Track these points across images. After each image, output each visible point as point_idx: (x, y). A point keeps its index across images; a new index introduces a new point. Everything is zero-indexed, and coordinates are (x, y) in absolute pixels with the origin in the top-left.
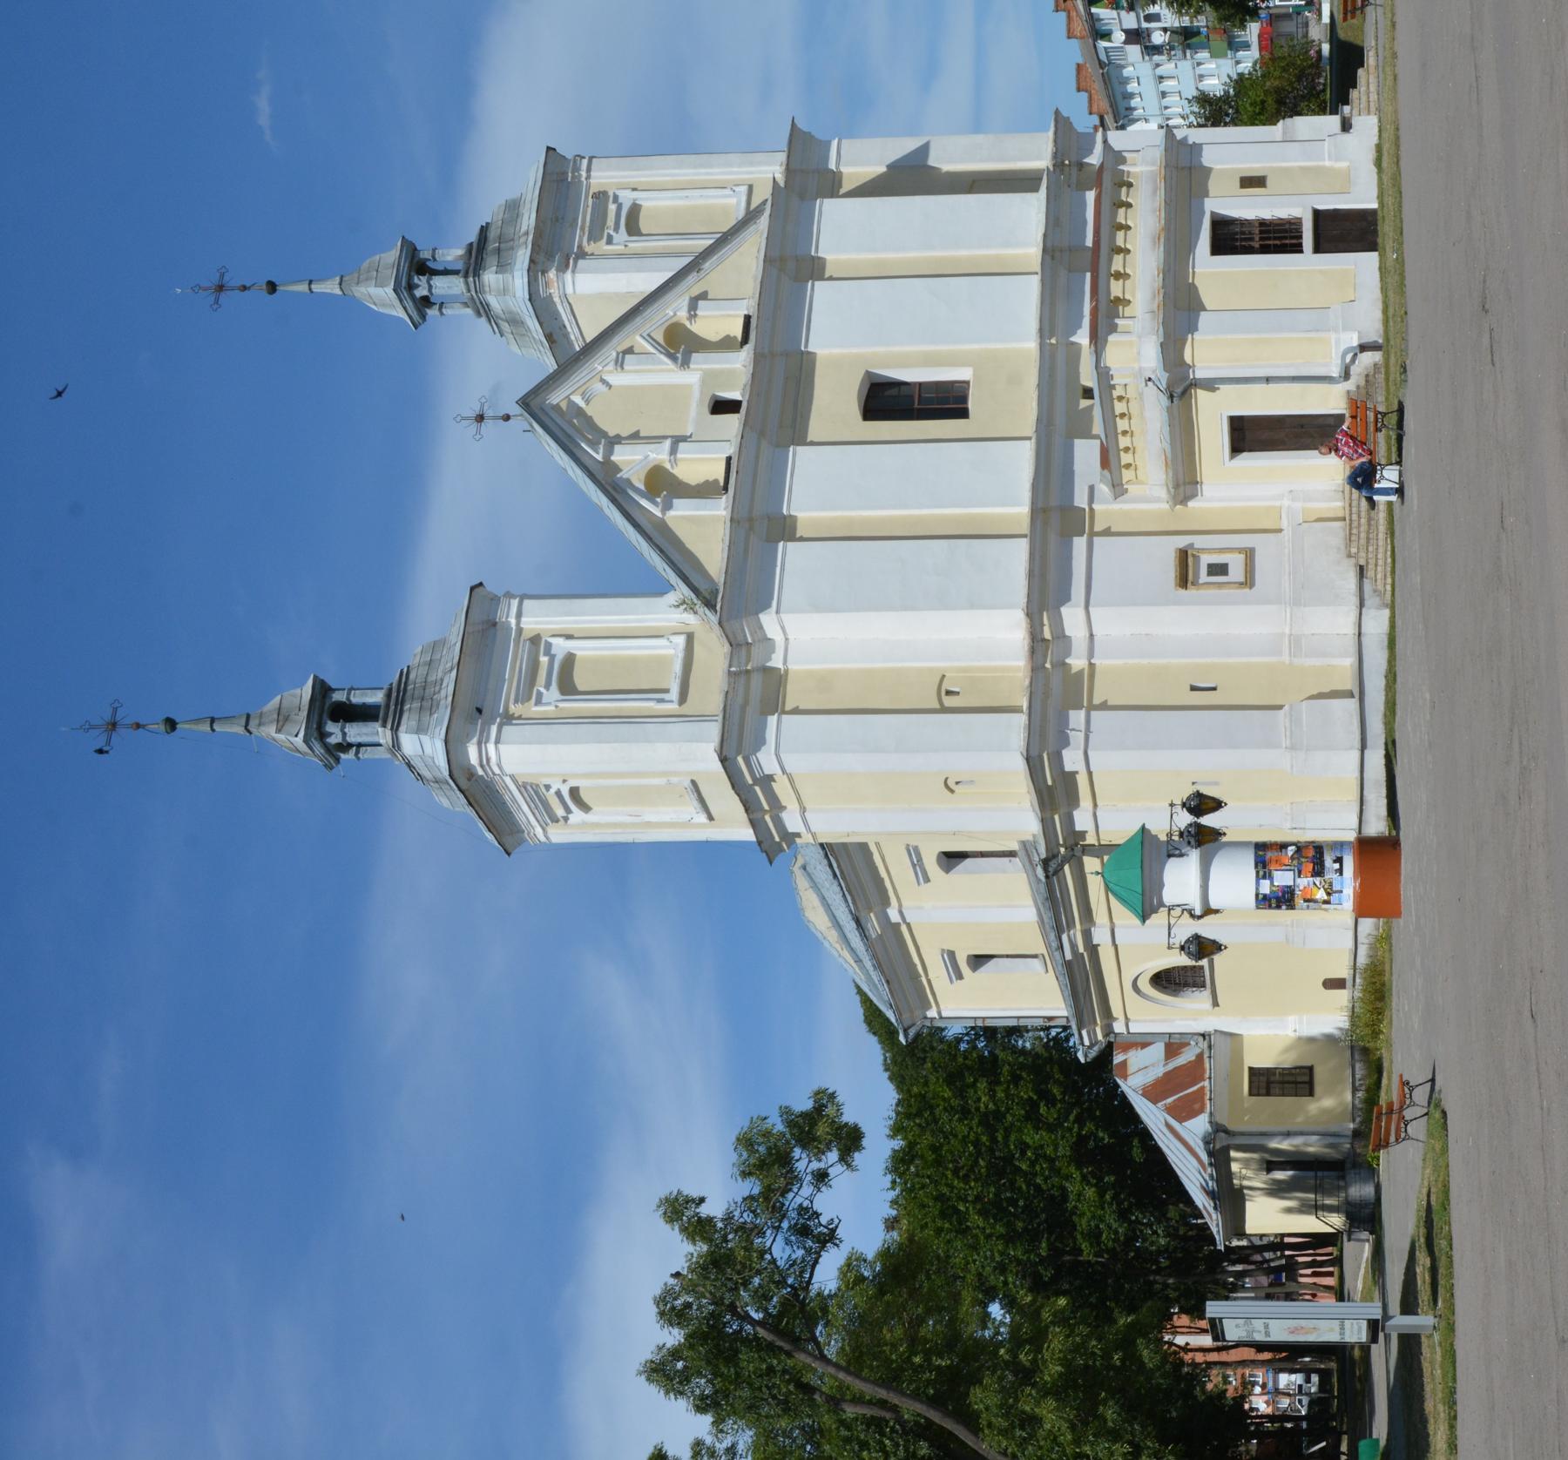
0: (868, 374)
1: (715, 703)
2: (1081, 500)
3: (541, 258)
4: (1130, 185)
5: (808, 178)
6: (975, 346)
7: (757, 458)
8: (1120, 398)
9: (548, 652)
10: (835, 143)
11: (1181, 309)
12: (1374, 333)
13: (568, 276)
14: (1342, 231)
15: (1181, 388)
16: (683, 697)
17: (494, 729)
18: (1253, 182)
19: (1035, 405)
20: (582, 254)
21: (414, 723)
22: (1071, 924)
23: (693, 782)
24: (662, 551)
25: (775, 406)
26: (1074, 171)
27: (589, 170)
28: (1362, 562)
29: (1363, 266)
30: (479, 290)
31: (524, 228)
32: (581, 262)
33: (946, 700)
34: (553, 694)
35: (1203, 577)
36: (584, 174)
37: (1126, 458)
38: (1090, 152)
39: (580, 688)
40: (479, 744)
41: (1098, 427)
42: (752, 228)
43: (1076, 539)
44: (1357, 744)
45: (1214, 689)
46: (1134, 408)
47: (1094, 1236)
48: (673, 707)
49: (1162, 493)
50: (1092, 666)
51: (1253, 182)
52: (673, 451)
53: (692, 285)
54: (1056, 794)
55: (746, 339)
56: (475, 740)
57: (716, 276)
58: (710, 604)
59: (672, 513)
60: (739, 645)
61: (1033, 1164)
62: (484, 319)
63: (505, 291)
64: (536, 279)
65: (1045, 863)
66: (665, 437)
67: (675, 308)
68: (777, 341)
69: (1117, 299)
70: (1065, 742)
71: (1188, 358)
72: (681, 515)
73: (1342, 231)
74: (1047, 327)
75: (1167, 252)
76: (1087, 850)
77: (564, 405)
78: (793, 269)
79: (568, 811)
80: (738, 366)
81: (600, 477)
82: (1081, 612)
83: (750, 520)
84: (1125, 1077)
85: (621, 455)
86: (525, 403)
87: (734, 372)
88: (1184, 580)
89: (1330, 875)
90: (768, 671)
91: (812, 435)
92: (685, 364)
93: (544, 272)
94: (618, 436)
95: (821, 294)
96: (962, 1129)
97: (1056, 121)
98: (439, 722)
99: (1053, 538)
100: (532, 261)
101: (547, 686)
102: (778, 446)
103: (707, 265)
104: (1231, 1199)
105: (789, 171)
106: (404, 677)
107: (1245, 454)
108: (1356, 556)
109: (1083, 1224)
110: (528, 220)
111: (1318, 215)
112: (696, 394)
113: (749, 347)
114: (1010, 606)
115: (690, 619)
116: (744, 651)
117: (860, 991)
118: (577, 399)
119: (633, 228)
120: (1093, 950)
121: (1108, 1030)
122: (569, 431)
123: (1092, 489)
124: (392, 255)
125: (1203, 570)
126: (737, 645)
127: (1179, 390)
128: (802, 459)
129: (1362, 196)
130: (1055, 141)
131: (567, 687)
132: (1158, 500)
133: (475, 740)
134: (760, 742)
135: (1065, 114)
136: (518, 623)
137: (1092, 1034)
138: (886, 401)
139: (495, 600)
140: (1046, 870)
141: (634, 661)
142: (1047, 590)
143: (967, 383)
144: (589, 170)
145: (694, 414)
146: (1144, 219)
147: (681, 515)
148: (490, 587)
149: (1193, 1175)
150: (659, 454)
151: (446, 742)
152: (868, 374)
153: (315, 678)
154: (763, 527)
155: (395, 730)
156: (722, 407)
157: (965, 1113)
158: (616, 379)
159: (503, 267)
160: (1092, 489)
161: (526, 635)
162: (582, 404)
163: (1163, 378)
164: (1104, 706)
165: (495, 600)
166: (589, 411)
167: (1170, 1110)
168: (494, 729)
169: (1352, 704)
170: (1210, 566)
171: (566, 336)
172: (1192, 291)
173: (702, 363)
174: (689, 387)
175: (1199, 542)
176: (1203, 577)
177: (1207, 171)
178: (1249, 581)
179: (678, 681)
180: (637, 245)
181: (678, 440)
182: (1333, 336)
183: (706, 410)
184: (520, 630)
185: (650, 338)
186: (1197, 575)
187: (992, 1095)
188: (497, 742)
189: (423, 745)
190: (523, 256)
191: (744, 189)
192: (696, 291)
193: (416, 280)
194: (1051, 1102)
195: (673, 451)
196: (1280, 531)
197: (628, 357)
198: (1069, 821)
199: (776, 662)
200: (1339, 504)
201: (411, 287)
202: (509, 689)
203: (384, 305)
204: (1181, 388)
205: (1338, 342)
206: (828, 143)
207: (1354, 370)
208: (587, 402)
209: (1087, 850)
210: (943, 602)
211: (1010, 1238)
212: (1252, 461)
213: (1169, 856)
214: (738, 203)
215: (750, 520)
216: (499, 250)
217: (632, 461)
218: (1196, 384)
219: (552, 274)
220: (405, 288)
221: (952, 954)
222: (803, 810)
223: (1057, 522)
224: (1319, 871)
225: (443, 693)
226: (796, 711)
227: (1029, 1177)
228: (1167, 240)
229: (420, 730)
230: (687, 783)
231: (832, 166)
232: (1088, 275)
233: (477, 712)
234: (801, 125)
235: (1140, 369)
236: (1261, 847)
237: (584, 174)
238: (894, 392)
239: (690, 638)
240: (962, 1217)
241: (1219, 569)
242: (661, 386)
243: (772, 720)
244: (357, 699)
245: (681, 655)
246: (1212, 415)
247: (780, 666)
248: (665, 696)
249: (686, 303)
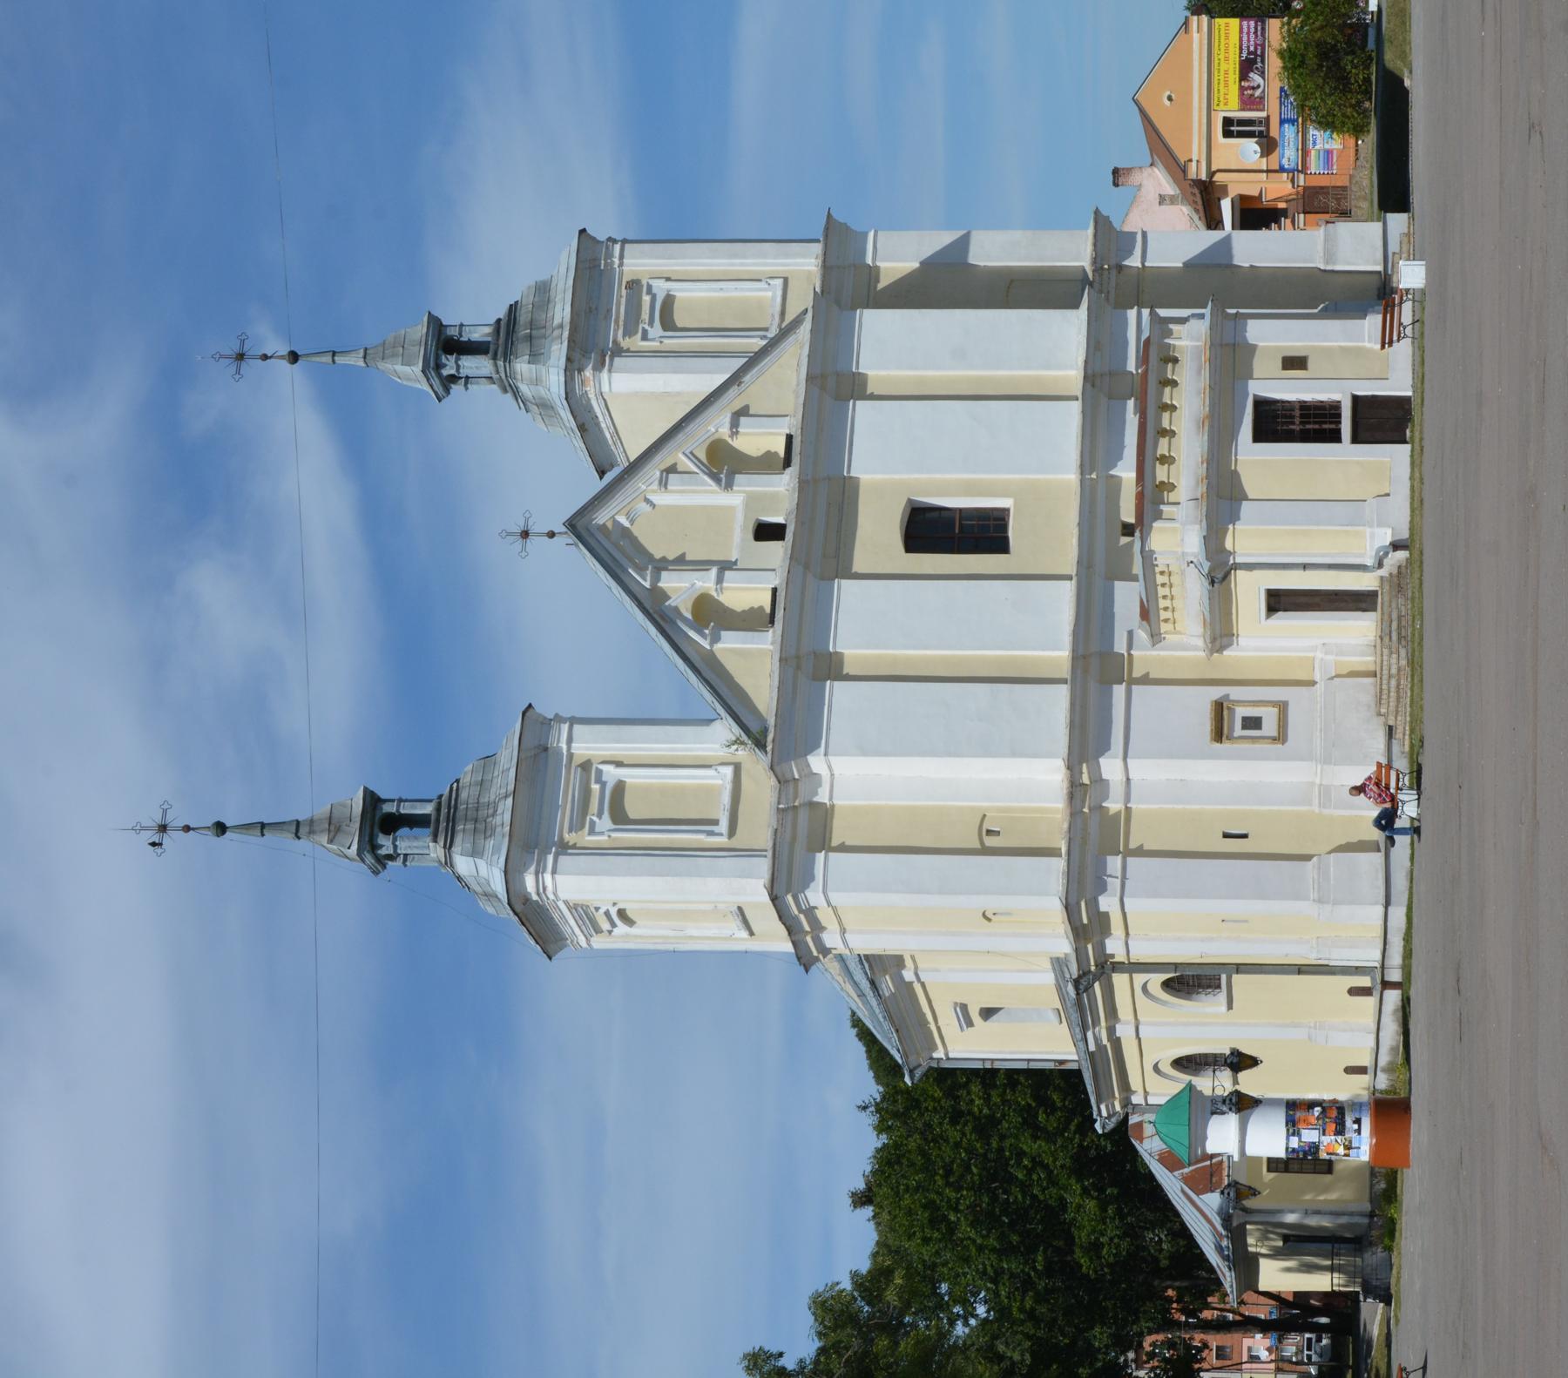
0: (910, 501)
1: (764, 840)
2: (1120, 646)
3: (577, 355)
4: (1175, 361)
5: (848, 287)
6: (1017, 476)
7: (803, 593)
8: (1162, 573)
9: (599, 780)
10: (871, 234)
11: (1224, 496)
12: (1405, 534)
13: (605, 375)
14: (1381, 420)
15: (1220, 572)
16: (732, 831)
17: (550, 858)
18: (1295, 363)
19: (1076, 531)
20: (618, 351)
21: (468, 846)
22: (1096, 1022)
23: (740, 909)
24: (711, 687)
25: (817, 539)
26: (1114, 272)
27: (621, 257)
28: (1391, 723)
29: (1395, 457)
30: (510, 375)
31: (557, 321)
32: (617, 360)
33: (988, 842)
34: (605, 823)
35: (1238, 731)
36: (616, 261)
37: (1163, 615)
38: (1130, 253)
39: (632, 815)
40: (537, 874)
41: (1137, 568)
42: (791, 339)
43: (1116, 687)
44: (1382, 899)
45: (1245, 836)
46: (1175, 579)
47: (1094, 1248)
48: (722, 841)
49: (1200, 643)
50: (1128, 809)
51: (1295, 363)
52: (720, 580)
53: (733, 400)
54: (1087, 927)
55: (787, 462)
56: (533, 869)
57: (755, 390)
58: (760, 744)
59: (718, 646)
60: (787, 781)
61: (1030, 1171)
62: (509, 396)
63: (537, 381)
64: (573, 379)
65: (1076, 983)
66: (711, 563)
67: (717, 424)
68: (818, 455)
69: (1162, 483)
70: (1102, 888)
71: (1228, 545)
72: (730, 646)
73: (1381, 420)
74: (1088, 462)
75: (1212, 405)
76: (1118, 967)
77: (609, 525)
78: (835, 387)
79: (613, 925)
80: (782, 489)
81: (648, 606)
82: (1119, 763)
83: (798, 657)
84: (1141, 1140)
85: (671, 582)
86: (572, 525)
87: (778, 495)
88: (1219, 734)
89: (1350, 1134)
90: (813, 806)
91: (858, 566)
92: (729, 486)
93: (580, 370)
94: (664, 559)
95: (864, 414)
96: (954, 1134)
97: (1096, 222)
98: (496, 850)
99: (1093, 686)
100: (569, 359)
101: (600, 815)
102: (823, 579)
103: (747, 378)
104: (1246, 1266)
105: (827, 268)
106: (455, 791)
107: (1280, 614)
108: (1386, 716)
109: (1082, 1236)
110: (561, 312)
111: (1356, 400)
112: (740, 517)
113: (793, 471)
114: (1050, 755)
115: (743, 754)
116: (791, 785)
117: (866, 1036)
118: (623, 520)
119: (668, 324)
120: (1117, 1043)
121: (1126, 1103)
122: (615, 553)
123: (1130, 633)
124: (420, 330)
125: (1238, 723)
126: (783, 781)
127: (1220, 576)
128: (848, 593)
129: (1397, 383)
130: (1095, 245)
131: (619, 816)
132: (1195, 648)
133: (533, 869)
134: (809, 878)
135: (1105, 213)
136: (569, 748)
137: (1110, 1107)
138: (930, 530)
139: (546, 724)
140: (1077, 988)
141: (683, 788)
142: (1088, 738)
143: (1007, 510)
144: (621, 257)
146: (1189, 398)
147: (730, 646)
148: (539, 708)
149: (1207, 1237)
150: (705, 582)
151: (506, 873)
152: (910, 501)
153: (366, 789)
154: (812, 665)
155: (448, 847)
156: (767, 532)
157: (956, 1117)
158: (660, 499)
159: (535, 357)
160: (1130, 633)
161: (577, 761)
162: (627, 524)
163: (1207, 565)
164: (1140, 852)
165: (546, 724)
166: (636, 531)
167: (1187, 1180)
168: (550, 858)
169: (1378, 858)
170: (1245, 719)
171: (598, 424)
172: (1235, 475)
173: (747, 485)
174: (732, 509)
175: (1235, 693)
176: (1238, 731)
177: (1252, 349)
178: (1281, 737)
179: (727, 814)
180: (672, 343)
181: (725, 566)
182: (1368, 530)
183: (751, 536)
184: (570, 756)
185: (692, 456)
186: (1232, 729)
187: (987, 1099)
188: (554, 872)
189: (482, 869)
190: (558, 352)
191: (779, 282)
192: (737, 405)
193: (444, 360)
194: (1051, 1108)
195: (720, 580)
196: (1313, 683)
197: (671, 476)
198: (1100, 947)
199: (822, 797)
200: (1371, 658)
201: (439, 366)
202: (564, 817)
203: (409, 379)
204: (1220, 572)
205: (1372, 536)
206: (865, 235)
207: (1386, 561)
208: (632, 522)
209: (1118, 967)
210: (986, 749)
211: (1005, 1251)
212: (1287, 621)
213: (1213, 1113)
214: (774, 298)
215: (798, 657)
216: (530, 338)
217: (680, 588)
218: (1237, 566)
219: (588, 373)
220: (432, 367)
221: (964, 1007)
222: (843, 931)
223: (1097, 669)
224: (1340, 1131)
225: (498, 819)
226: (843, 848)
227: (1025, 1187)
228: (1211, 427)
229: (475, 853)
230: (735, 908)
231: (869, 261)
232: (1131, 403)
233: (533, 841)
234: (838, 216)
235: (1183, 553)
236: (1292, 1105)
237: (616, 261)
238: (935, 515)
239: (737, 768)
240: (952, 1229)
241: (1253, 723)
242: (704, 507)
243: (820, 857)
244: (406, 809)
245: (729, 787)
246: (1249, 591)
247: (826, 801)
248: (715, 829)
249: (727, 419)
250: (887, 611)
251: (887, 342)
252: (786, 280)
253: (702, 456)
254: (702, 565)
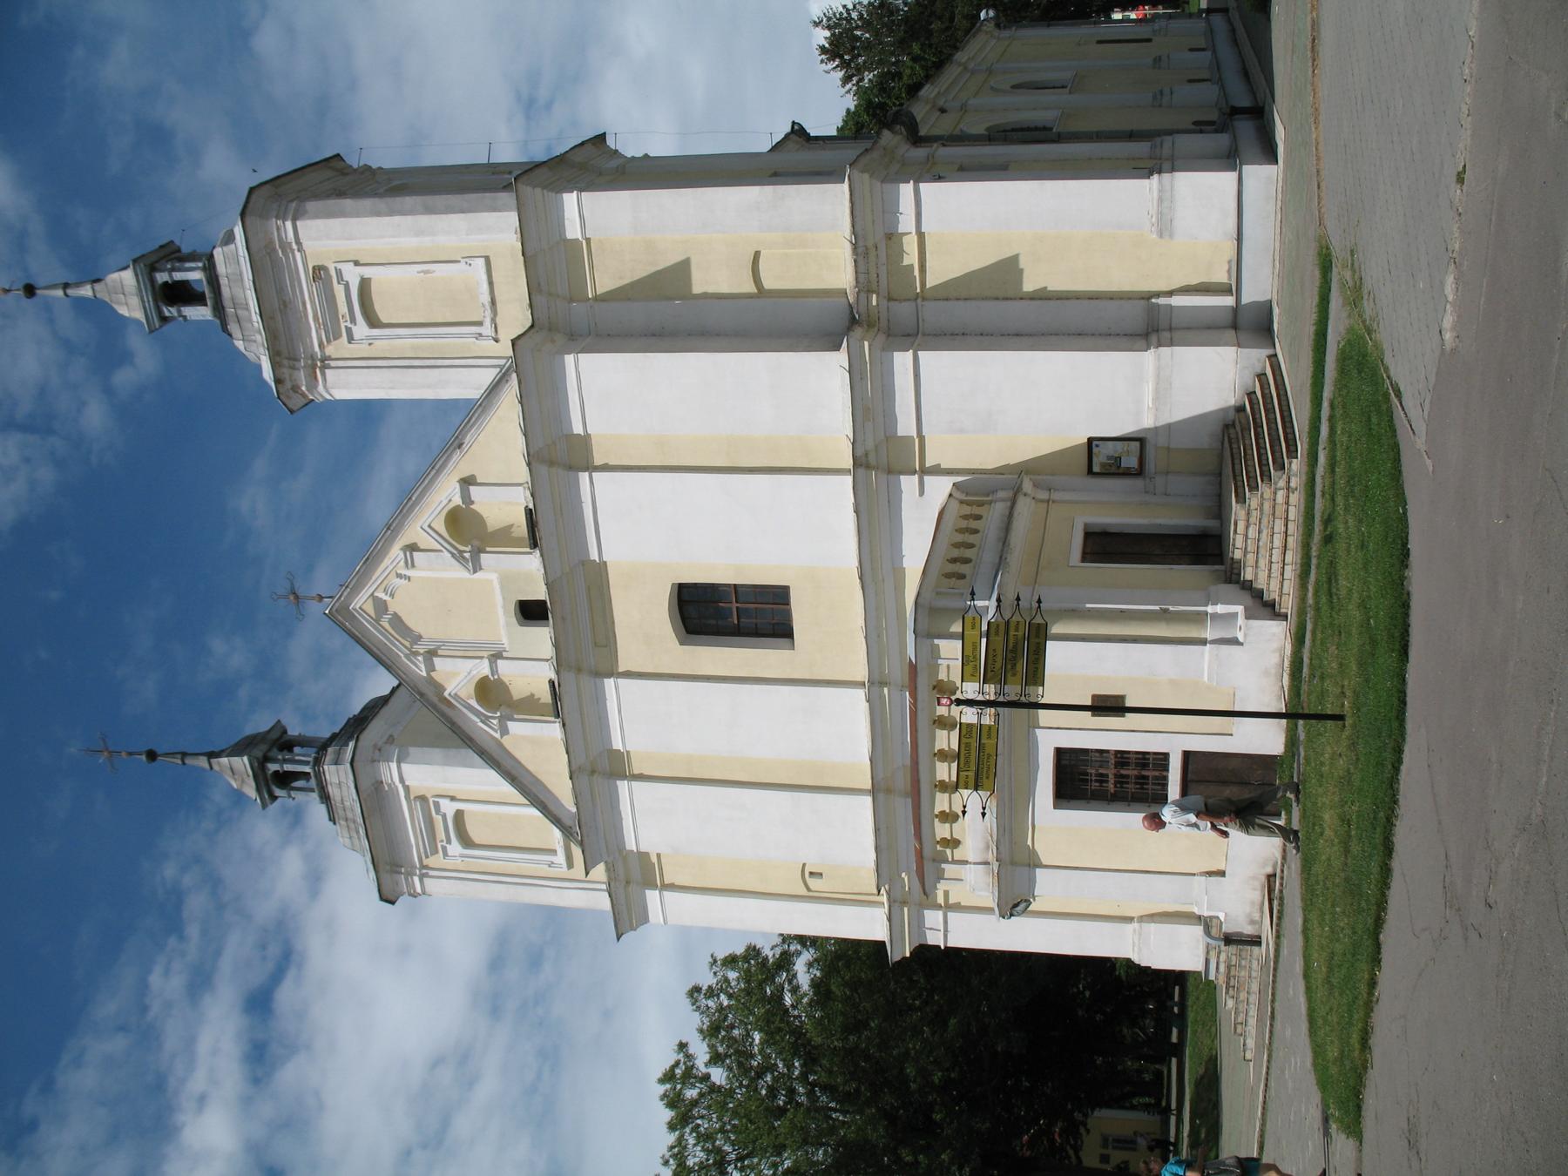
111: (1187, 755)
145: (504, 627)
180: (385, 343)
191: (481, 262)
250: (670, 707)
251: (611, 392)
252: (487, 259)
253: (442, 530)
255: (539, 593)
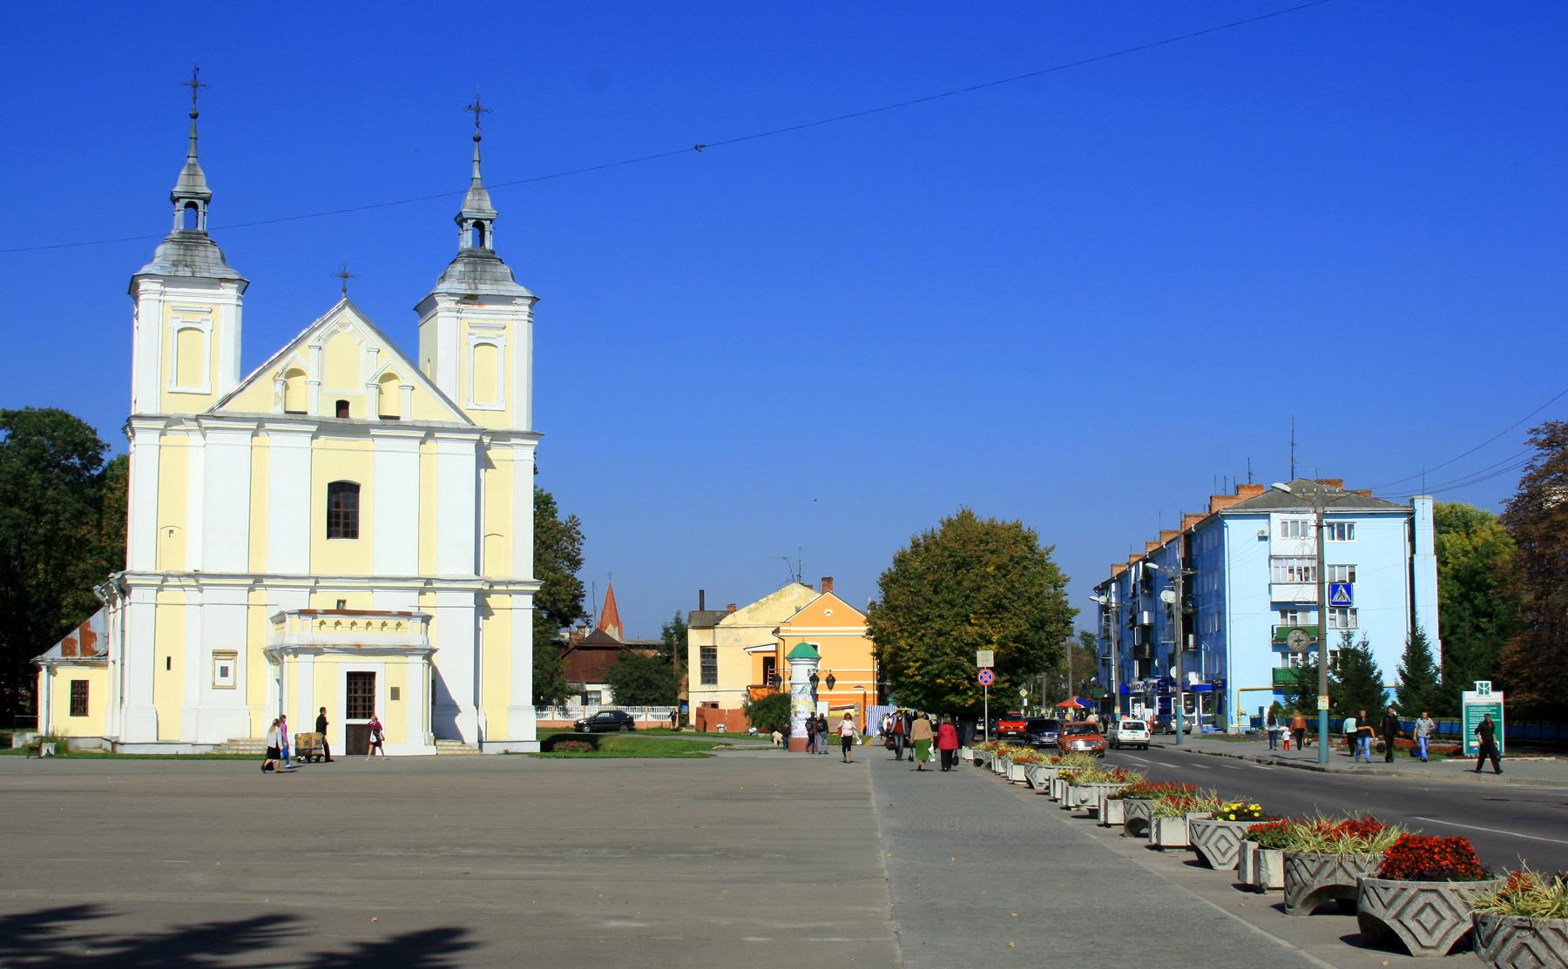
14: (362, 739)
18: (395, 694)
51: (395, 694)
88: (217, 653)
125: (224, 664)
178: (215, 687)
241: (224, 672)
254: (321, 369)
255: (355, 413)
